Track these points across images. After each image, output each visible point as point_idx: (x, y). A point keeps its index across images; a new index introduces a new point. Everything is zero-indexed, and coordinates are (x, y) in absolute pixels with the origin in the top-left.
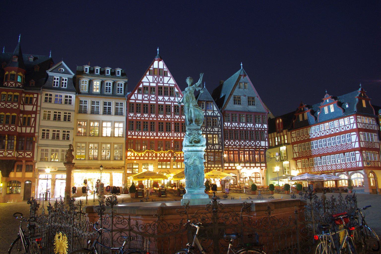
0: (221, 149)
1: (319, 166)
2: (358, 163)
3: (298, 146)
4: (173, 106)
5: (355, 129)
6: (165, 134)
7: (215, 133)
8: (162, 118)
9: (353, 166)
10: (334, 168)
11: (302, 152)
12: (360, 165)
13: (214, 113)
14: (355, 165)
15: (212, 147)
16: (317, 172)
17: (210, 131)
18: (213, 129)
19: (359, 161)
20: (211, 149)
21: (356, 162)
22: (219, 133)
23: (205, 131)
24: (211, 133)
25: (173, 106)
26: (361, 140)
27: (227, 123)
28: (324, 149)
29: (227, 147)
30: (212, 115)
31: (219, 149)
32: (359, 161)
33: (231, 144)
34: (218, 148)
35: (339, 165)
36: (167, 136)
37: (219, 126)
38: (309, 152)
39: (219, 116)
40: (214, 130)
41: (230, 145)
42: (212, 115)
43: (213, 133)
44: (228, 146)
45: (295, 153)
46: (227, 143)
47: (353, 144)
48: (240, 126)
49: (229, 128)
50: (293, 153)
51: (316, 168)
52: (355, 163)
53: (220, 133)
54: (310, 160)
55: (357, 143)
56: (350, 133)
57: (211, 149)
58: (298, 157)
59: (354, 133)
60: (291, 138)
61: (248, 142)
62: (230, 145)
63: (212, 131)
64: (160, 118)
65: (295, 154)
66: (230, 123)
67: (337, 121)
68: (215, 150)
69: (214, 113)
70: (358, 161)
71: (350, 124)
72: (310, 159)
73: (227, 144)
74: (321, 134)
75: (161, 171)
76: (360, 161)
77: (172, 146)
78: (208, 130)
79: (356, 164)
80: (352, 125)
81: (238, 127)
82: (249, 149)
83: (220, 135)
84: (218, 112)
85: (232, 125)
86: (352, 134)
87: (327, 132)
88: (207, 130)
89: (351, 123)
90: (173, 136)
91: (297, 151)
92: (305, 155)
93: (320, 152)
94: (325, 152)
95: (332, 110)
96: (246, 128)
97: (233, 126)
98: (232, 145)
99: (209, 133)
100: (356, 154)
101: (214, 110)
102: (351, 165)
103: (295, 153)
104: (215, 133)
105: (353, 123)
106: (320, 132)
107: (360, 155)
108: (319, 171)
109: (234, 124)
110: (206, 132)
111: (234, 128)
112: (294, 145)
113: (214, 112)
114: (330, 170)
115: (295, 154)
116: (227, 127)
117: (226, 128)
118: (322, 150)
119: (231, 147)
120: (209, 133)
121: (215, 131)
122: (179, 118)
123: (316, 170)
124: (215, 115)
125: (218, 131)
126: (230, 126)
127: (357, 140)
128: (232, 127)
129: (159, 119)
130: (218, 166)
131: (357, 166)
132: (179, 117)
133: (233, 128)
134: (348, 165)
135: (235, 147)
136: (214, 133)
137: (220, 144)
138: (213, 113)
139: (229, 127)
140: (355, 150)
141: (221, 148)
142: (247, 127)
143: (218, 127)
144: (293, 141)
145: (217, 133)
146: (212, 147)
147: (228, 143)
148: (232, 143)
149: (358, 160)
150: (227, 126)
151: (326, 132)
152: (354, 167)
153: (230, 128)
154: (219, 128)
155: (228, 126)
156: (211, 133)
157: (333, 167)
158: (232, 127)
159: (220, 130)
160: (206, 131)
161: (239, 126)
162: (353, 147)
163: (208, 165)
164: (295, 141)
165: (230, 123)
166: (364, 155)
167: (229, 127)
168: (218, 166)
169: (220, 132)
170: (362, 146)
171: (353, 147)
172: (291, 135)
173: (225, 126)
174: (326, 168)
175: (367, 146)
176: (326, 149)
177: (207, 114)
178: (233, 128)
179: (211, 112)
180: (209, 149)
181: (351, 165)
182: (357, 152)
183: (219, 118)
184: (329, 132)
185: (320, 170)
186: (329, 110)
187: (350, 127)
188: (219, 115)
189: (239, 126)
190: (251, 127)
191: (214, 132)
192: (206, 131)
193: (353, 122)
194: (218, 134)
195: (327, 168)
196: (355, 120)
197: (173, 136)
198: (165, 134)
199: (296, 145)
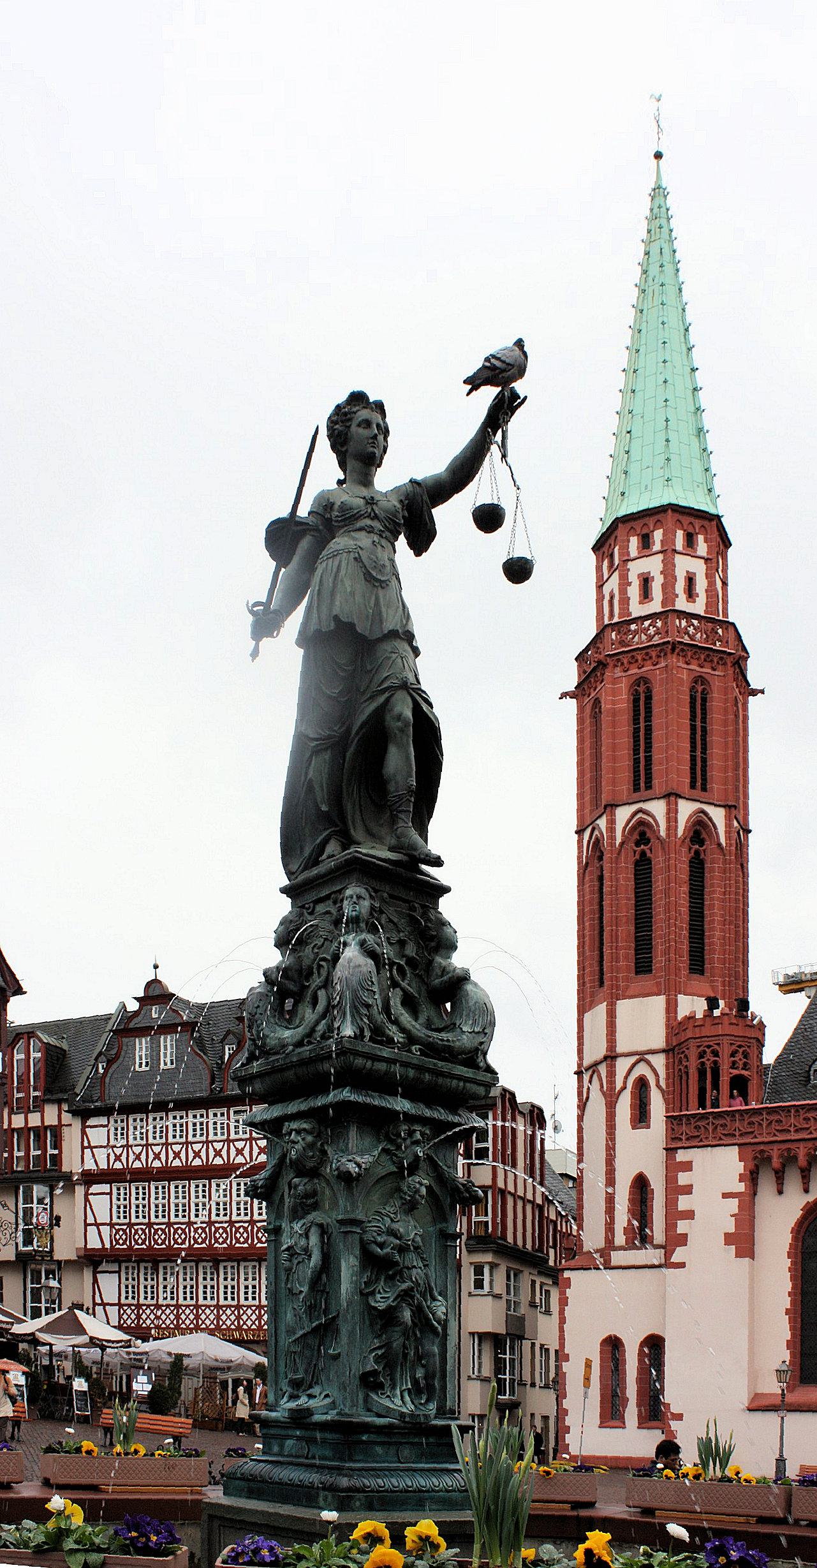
3: (110, 1194)
38: (163, 1231)
45: (97, 1225)
50: (86, 1225)
58: (108, 1246)
60: (83, 1148)
65: (92, 1230)
74: (233, 1152)
91: (103, 1217)
92: (144, 1242)
94: (238, 1241)
103: (97, 1225)
106: (229, 1141)
112: (95, 1188)
114: (249, 1329)
115: (92, 1230)
118: (225, 1229)
123: (187, 1322)
144: (90, 1165)
164: (103, 1165)
172: (84, 1133)
174: (233, 1317)
185: (208, 1322)
195: (239, 1318)
199: (106, 1188)
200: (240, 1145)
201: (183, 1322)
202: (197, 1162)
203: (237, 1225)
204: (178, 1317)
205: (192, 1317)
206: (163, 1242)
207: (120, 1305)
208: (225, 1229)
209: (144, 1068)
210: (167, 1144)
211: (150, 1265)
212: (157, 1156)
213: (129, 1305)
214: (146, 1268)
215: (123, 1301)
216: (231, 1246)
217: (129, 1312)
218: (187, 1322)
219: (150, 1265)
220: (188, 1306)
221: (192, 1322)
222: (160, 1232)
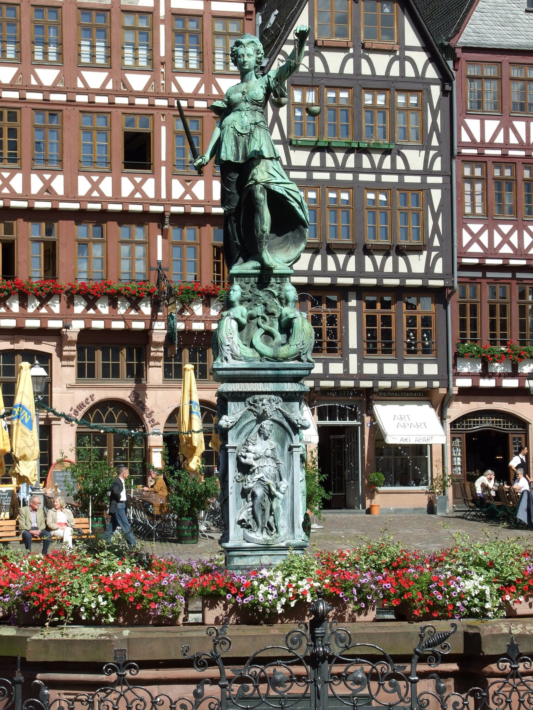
0: (437, 277)
4: (162, 13)
6: (117, 187)
7: (408, 179)
8: (101, 92)
13: (408, 64)
17: (378, 171)
18: (399, 159)
22: (431, 180)
25: (162, 13)
29: (476, 261)
30: (395, 72)
31: (429, 273)
33: (501, 245)
36: (131, 200)
37: (435, 142)
39: (433, 82)
40: (400, 165)
42: (395, 72)
46: (475, 238)
49: (487, 152)
53: (439, 180)
62: (491, 252)
63: (393, 171)
64: (87, 91)
66: (498, 122)
68: (403, 277)
69: (408, 64)
73: (475, 248)
75: (92, 396)
77: (160, 258)
78: (366, 163)
83: (436, 195)
85: (506, 137)
88: (359, 162)
90: (164, 196)
97: (513, 140)
98: (506, 249)
99: (372, 178)
101: (408, 43)
104: (408, 179)
110: (356, 177)
111: (522, 153)
113: (408, 53)
116: (482, 145)
120: (372, 178)
121: (409, 172)
122: (202, 91)
124: (410, 72)
125: (427, 172)
126: (500, 139)
128: (506, 146)
129: (82, 99)
132: (198, 87)
135: (523, 262)
137: (436, 243)
141: (439, 269)
143: (426, 147)
147: (484, 238)
148: (506, 239)
150: (478, 140)
153: (499, 152)
154: (432, 153)
155: (487, 140)
156: (385, 178)
158: (506, 146)
159: (437, 166)
160: (358, 170)
163: (360, 368)
165: (498, 122)
167: (492, 145)
168: (421, 369)
173: (465, 138)
177: (366, 70)
178: (511, 153)
180: (369, 276)
183: (436, 91)
188: (431, 73)
191: (401, 174)
192: (358, 170)
197: (164, 196)
198: (117, 187)
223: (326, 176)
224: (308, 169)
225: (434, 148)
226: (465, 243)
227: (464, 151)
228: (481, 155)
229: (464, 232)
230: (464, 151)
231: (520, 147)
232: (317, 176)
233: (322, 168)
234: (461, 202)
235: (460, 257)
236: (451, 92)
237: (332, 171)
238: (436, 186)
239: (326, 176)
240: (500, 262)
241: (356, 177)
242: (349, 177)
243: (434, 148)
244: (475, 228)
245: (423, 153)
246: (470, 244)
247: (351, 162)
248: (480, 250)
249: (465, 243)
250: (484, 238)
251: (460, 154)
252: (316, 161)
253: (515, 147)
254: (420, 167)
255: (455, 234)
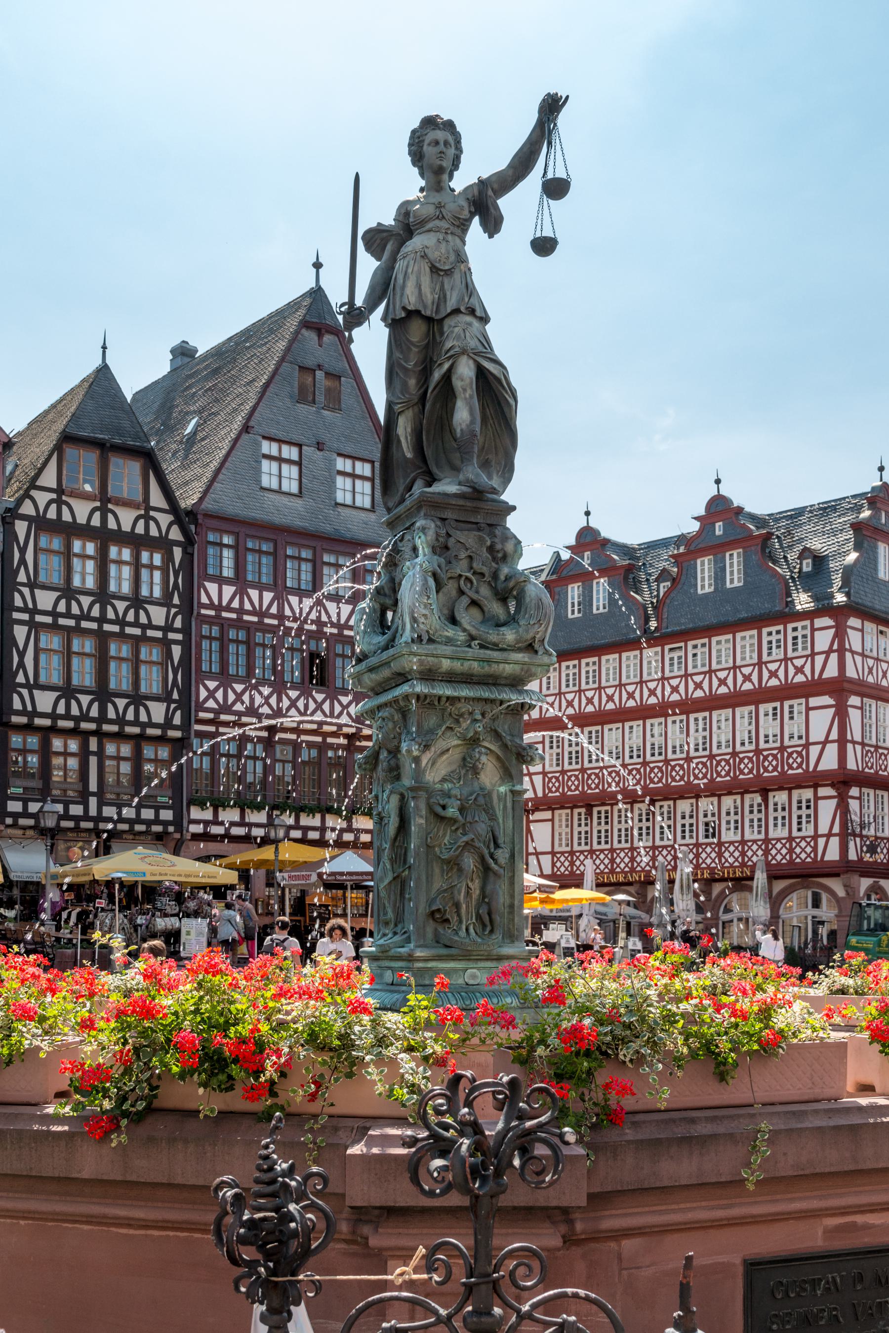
1: (596, 846)
2: (821, 842)
5: (831, 681)
7: (150, 633)
9: (798, 856)
10: (708, 861)
11: (563, 772)
12: (833, 854)
14: (809, 850)
15: (131, 709)
16: (626, 873)
19: (829, 835)
20: (121, 721)
21: (816, 837)
22: (172, 636)
23: (93, 619)
24: (129, 630)
26: (849, 737)
27: (216, 586)
28: (673, 768)
29: (211, 716)
32: (829, 835)
33: (234, 703)
34: (162, 721)
35: (732, 849)
37: (176, 600)
39: (177, 543)
40: (143, 619)
41: (226, 708)
43: (137, 631)
44: (217, 712)
46: (211, 694)
47: (814, 751)
48: (288, 612)
49: (225, 614)
51: (622, 855)
52: (809, 843)
53: (179, 637)
54: (595, 815)
55: (832, 750)
56: (807, 697)
57: (121, 721)
58: (540, 794)
59: (827, 700)
61: (324, 701)
63: (136, 624)
66: (234, 588)
67: (751, 637)
70: (822, 836)
71: (813, 654)
72: (599, 812)
73: (211, 704)
76: (835, 835)
78: (111, 615)
79: (815, 849)
80: (819, 660)
81: (273, 616)
82: (325, 735)
83: (177, 651)
84: (171, 518)
85: (242, 602)
86: (814, 701)
87: (698, 686)
88: (103, 611)
89: (816, 650)
92: (577, 788)
93: (652, 781)
94: (674, 779)
95: (735, 579)
96: (318, 622)
97: (248, 606)
98: (238, 707)
99: (116, 628)
100: (817, 798)
102: (791, 851)
104: (150, 633)
105: (828, 653)
107: (838, 806)
108: (636, 872)
109: (254, 594)
110: (100, 627)
116: (219, 608)
117: (212, 613)
118: (660, 769)
119: (232, 718)
120: (116, 628)
121: (150, 626)
123: (622, 865)
125: (168, 628)
126: (235, 604)
127: (834, 735)
128: (241, 611)
130: (157, 814)
131: (816, 855)
133: (246, 618)
134: (774, 852)
136: (144, 632)
137: (175, 696)
138: (147, 518)
139: (228, 609)
140: (814, 780)
142: (324, 618)
145: (159, 634)
146: (131, 709)
147: (219, 695)
149: (823, 829)
150: (216, 602)
151: (691, 686)
152: (803, 861)
153: (234, 616)
154: (173, 611)
155: (224, 603)
156: (129, 630)
157: (704, 855)
158: (241, 611)
159: (178, 623)
161: (281, 608)
162: (811, 769)
165: (234, 588)
166: (854, 805)
167: (228, 609)
169: (177, 631)
170: (851, 765)
171: (811, 769)
173: (204, 600)
175: (872, 768)
176: (682, 767)
178: (246, 618)
179: (134, 514)
181: (791, 851)
182: (823, 791)
184: (706, 685)
186: (720, 575)
187: (807, 669)
189: (281, 608)
190: (342, 621)
191: (144, 627)
192: (102, 619)
193: (826, 648)
194: (166, 644)
196: (836, 635)
200: (674, 682)
201: (618, 866)
202: (631, 703)
203: (673, 763)
204: (612, 861)
205: (627, 860)
206: (597, 787)
207: (553, 853)
208: (660, 769)
209: (576, 615)
210: (600, 688)
211: (583, 810)
212: (590, 701)
213: (563, 853)
214: (580, 814)
215: (557, 849)
216: (667, 785)
217: (562, 859)
218: (622, 865)
219: (583, 810)
220: (622, 849)
221: (627, 865)
222: (593, 777)
223: (71, 623)
224: (54, 614)
225: (175, 606)
226: (201, 699)
227: (203, 611)
228: (218, 616)
229: (201, 688)
230: (203, 611)
231: (253, 613)
232: (62, 621)
233: (68, 615)
234: (199, 660)
235: (197, 711)
236: (192, 555)
237: (78, 618)
238: (176, 642)
239: (71, 623)
240: (232, 718)
241: (100, 627)
242: (94, 626)
243: (175, 606)
244: (212, 685)
245: (165, 609)
246: (206, 700)
247: (96, 612)
248: (216, 706)
249: (201, 699)
250: (219, 695)
251: (199, 613)
252: (62, 607)
253: (249, 613)
254: (162, 623)
255: (193, 689)
